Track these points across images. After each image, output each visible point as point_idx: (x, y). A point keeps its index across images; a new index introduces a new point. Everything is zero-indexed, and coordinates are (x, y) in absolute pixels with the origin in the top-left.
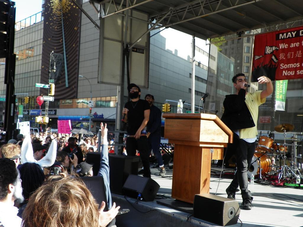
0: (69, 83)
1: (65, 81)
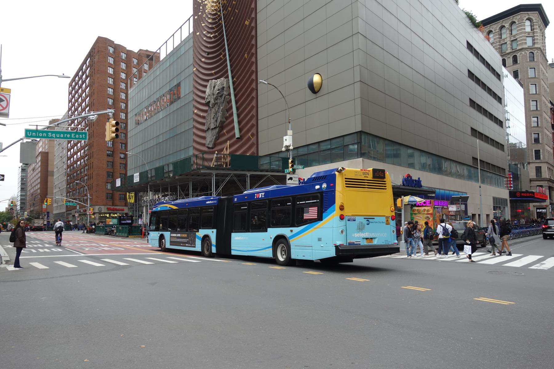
0: (240, 130)
1: (233, 128)
